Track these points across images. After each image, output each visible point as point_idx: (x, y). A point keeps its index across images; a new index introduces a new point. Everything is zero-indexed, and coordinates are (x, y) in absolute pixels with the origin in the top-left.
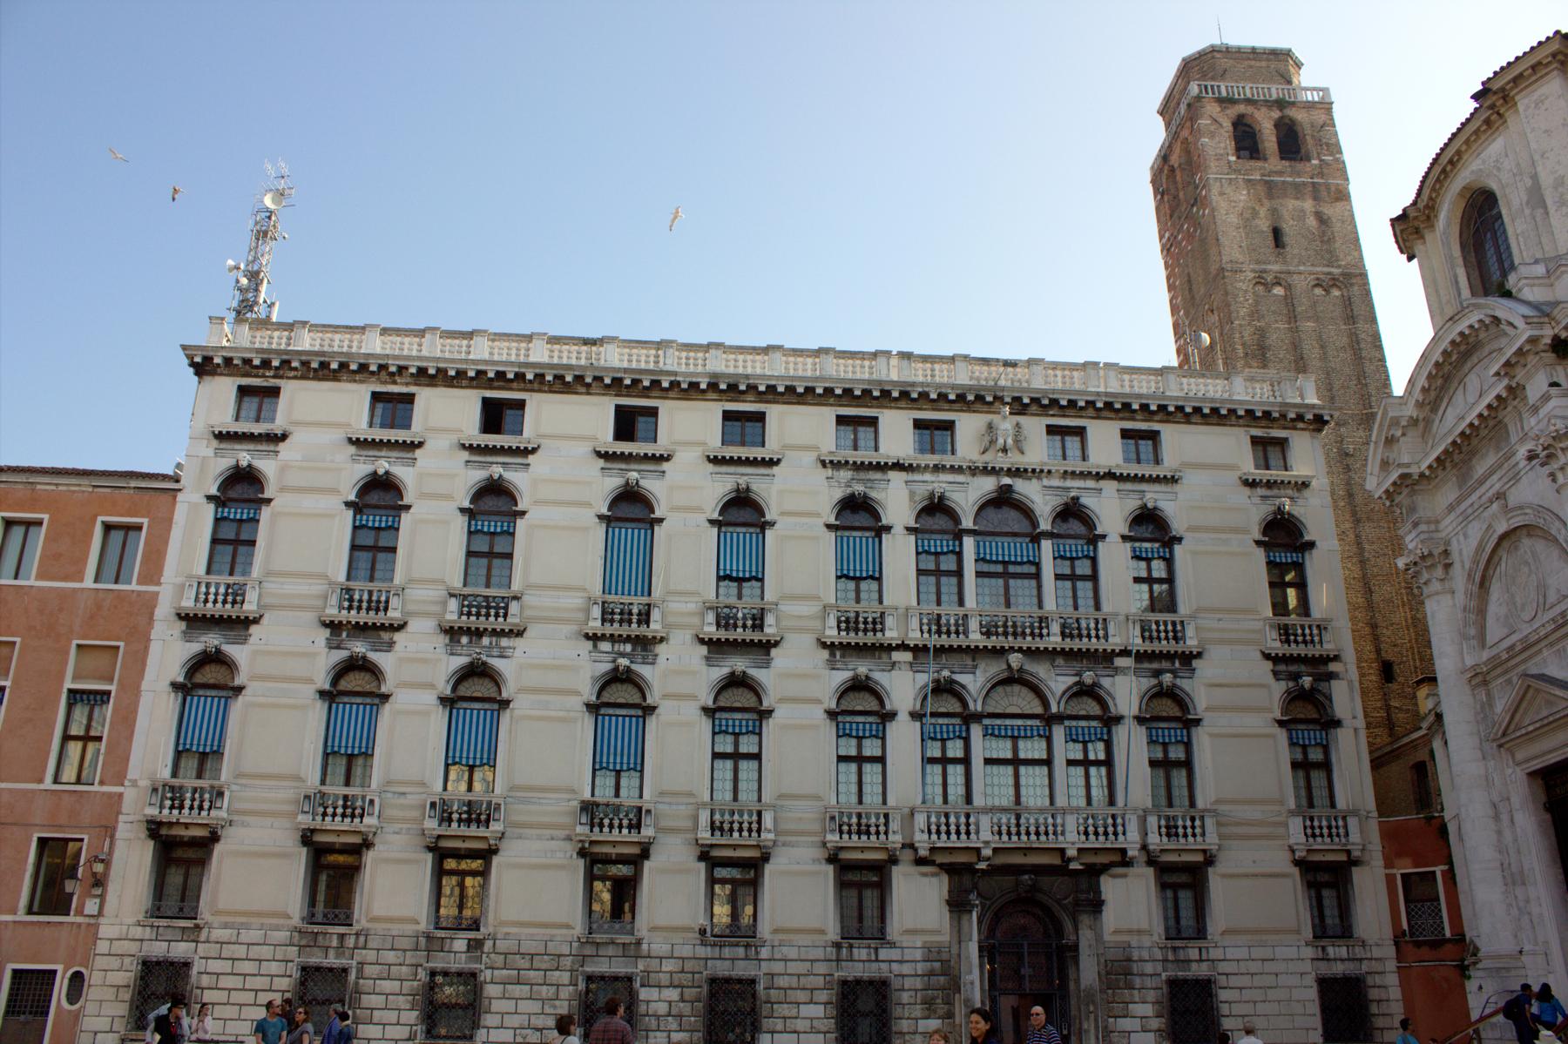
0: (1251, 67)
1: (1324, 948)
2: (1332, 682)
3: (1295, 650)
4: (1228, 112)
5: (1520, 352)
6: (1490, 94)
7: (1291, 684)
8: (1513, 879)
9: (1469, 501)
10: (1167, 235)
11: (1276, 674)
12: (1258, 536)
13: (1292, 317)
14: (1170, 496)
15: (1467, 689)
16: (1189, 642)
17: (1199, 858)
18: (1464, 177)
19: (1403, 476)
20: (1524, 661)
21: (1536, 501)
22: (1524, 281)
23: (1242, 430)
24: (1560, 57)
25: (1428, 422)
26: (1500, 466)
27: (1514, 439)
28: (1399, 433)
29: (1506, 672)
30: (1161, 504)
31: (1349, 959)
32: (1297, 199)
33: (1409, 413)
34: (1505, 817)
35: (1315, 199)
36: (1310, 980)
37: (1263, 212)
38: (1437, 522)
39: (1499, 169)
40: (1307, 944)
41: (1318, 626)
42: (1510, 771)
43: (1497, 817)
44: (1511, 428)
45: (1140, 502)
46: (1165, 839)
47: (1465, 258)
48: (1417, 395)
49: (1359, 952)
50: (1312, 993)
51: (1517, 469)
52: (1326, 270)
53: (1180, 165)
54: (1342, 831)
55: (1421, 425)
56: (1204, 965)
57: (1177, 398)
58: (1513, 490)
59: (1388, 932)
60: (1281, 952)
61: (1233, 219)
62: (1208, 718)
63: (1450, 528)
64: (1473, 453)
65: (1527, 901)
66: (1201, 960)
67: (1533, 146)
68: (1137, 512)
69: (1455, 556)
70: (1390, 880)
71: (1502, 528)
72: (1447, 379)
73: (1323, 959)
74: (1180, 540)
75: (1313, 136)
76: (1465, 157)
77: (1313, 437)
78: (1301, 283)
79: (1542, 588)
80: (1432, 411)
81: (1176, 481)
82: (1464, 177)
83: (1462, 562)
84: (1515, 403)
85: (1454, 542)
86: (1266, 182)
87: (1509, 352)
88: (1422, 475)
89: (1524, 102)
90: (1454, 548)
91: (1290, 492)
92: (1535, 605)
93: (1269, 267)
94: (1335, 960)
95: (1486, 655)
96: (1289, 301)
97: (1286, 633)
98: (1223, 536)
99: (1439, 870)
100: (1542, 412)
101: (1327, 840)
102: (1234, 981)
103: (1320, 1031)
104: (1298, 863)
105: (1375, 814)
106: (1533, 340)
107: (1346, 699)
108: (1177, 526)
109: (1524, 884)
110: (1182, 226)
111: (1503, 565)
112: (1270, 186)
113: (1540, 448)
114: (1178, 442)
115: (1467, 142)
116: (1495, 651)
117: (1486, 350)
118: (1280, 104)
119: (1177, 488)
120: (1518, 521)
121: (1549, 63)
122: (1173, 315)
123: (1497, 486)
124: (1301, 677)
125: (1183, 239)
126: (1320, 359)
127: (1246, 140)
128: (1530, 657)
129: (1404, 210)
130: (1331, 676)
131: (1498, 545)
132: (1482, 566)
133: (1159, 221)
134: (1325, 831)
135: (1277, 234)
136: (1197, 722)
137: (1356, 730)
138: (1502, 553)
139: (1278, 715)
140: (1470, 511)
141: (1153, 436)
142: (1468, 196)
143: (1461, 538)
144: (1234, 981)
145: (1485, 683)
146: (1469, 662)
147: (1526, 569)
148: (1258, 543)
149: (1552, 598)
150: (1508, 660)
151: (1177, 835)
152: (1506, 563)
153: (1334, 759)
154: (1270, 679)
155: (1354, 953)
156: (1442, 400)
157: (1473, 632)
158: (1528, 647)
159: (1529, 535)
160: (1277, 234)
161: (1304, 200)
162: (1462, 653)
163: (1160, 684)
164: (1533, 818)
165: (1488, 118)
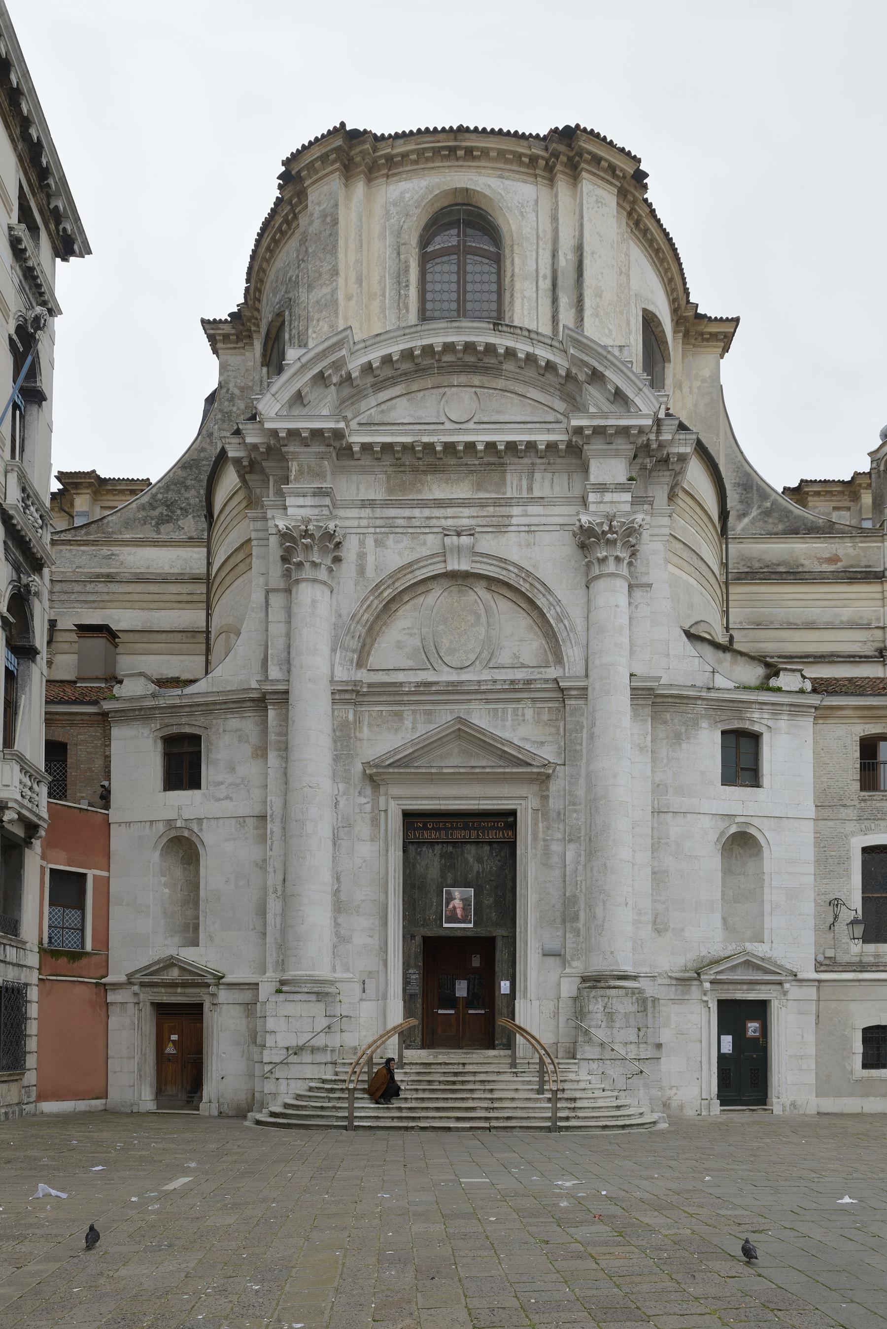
8: (339, 907)
9: (407, 513)
15: (330, 697)
25: (358, 395)
26: (482, 506)
55: (347, 391)
63: (355, 523)
70: (42, 868)
72: (421, 371)
92: (473, 657)
94: (9, 963)
123: (465, 522)
131: (434, 578)
132: (401, 585)
140: (401, 522)
146: (341, 674)
147: (471, 618)
149: (504, 658)
158: (454, 690)
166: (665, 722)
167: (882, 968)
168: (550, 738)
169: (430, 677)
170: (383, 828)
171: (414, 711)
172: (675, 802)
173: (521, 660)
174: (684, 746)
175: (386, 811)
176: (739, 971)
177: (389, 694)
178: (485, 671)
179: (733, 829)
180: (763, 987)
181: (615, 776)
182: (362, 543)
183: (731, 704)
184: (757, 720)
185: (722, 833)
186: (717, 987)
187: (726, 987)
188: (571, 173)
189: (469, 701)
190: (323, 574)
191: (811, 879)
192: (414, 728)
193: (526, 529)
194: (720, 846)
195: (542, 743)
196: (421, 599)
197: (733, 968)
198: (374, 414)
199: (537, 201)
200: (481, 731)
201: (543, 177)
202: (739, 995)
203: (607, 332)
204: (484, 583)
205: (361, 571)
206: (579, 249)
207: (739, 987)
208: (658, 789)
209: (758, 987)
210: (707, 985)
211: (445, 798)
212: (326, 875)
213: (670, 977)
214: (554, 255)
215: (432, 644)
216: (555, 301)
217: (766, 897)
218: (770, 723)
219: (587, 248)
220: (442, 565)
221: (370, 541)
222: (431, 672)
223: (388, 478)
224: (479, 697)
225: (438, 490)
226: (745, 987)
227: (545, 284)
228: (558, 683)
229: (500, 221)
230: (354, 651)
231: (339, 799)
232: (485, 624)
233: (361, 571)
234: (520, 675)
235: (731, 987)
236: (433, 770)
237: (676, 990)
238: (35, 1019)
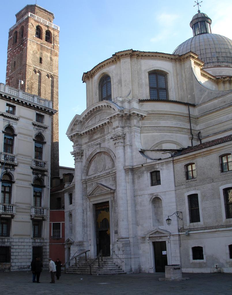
0: (43, 14)
1: (35, 240)
2: (45, 177)
3: (39, 168)
4: (36, 24)
5: (115, 116)
6: (115, 56)
7: (36, 176)
8: (85, 226)
9: (91, 143)
10: (10, 49)
11: (33, 173)
12: (34, 138)
13: (40, 82)
14: (16, 124)
16: (15, 162)
17: (10, 216)
18: (105, 70)
19: (77, 134)
20: (97, 180)
22: (118, 101)
23: (34, 111)
24: (131, 54)
25: (84, 123)
26: (101, 138)
28: (78, 123)
29: (92, 182)
30: (13, 125)
31: (40, 242)
32: (47, 52)
33: (81, 120)
34: (85, 213)
35: (51, 54)
36: (31, 247)
37: (39, 53)
38: (81, 145)
39: (112, 72)
40: (32, 239)
41: (44, 163)
43: (83, 213)
44: (105, 130)
45: (8, 124)
46: (3, 211)
47: (99, 88)
48: (84, 116)
49: (42, 241)
50: (31, 250)
52: (50, 72)
53: (19, 32)
54: (11, 210)
56: (8, 243)
57: (22, 99)
58: (102, 143)
59: (48, 236)
60: (26, 240)
61: (31, 52)
62: (16, 181)
63: (85, 148)
64: (94, 133)
65: (87, 231)
66: (8, 242)
67: (122, 71)
68: (7, 126)
69: (84, 154)
70: (50, 224)
71: (98, 151)
72: (92, 114)
73: (34, 242)
74: (16, 135)
75: (54, 38)
76: (105, 66)
77: (50, 117)
78: (44, 74)
79: (105, 166)
80: (86, 120)
81: (47, 128)
82: (105, 70)
83: (86, 156)
84: (108, 125)
85: (85, 151)
86: (41, 45)
87: (112, 115)
88: (81, 134)
89: (122, 61)
90: (85, 152)
91: (42, 129)
93: (37, 67)
94: (37, 242)
95: (88, 177)
96: (40, 77)
97: (37, 163)
98: (26, 137)
99: (61, 223)
100: (116, 130)
101: (39, 214)
102: (15, 247)
103: (32, 259)
104: (32, 219)
105: (49, 209)
106: (118, 114)
107: (47, 181)
108: (16, 132)
109: (87, 227)
110: (16, 48)
111: (96, 159)
112: (42, 47)
113: (114, 137)
114: (20, 110)
115: (107, 63)
116: (90, 177)
117: (103, 111)
118: (48, 27)
119: (17, 122)
120: (102, 150)
122: (7, 70)
123: (99, 142)
124: (39, 174)
125: (15, 52)
126: (44, 94)
127: (39, 33)
128: (98, 180)
129: (87, 72)
130: (45, 175)
132: (91, 158)
133: (9, 44)
134: (39, 212)
135: (41, 59)
136: (14, 182)
137: (48, 189)
138: (97, 156)
139: (32, 183)
140: (91, 145)
141: (14, 107)
143: (87, 150)
144: (15, 247)
145: (86, 183)
146: (83, 178)
148: (34, 140)
149: (107, 168)
150: (93, 179)
151: (6, 210)
152: (97, 158)
153: (42, 195)
154: (32, 174)
155: (41, 241)
156: (89, 119)
157: (85, 171)
159: (104, 154)
160: (41, 59)
161: (48, 53)
162: (82, 177)
163: (7, 171)
164: (92, 214)
165: (113, 60)
166: (136, 174)
167: (195, 230)
168: (114, 184)
169: (96, 175)
172: (139, 193)
174: (141, 179)
176: (157, 233)
179: (154, 197)
180: (163, 238)
183: (151, 166)
184: (158, 168)
185: (151, 198)
186: (151, 238)
187: (154, 238)
189: (102, 179)
191: (175, 207)
193: (108, 140)
194: (151, 202)
195: (113, 185)
197: (155, 233)
198: (87, 126)
202: (157, 240)
207: (157, 238)
208: (134, 191)
209: (162, 238)
210: (148, 238)
211: (98, 200)
212: (81, 220)
213: (141, 237)
217: (163, 213)
218: (161, 168)
223: (89, 137)
226: (159, 238)
235: (155, 238)
237: (142, 240)
238: (48, 252)
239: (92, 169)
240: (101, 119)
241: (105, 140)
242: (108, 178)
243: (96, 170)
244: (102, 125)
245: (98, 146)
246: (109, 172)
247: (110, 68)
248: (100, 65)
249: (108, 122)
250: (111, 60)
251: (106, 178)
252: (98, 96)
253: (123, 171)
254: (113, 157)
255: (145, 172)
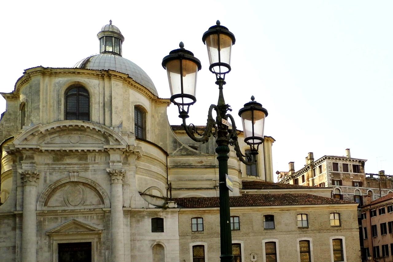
21: (93, 179)
27: (89, 161)
39: (95, 88)
42: (47, 241)
51: (88, 169)
84: (97, 154)
100: (115, 164)
106: (123, 148)
113: (114, 172)
115: (88, 74)
117: (86, 134)
121: (122, 79)
123: (76, 168)
142: (77, 83)
147: (78, 193)
149: (88, 203)
152: (67, 187)
158: (73, 211)
159: (83, 185)
169: (66, 208)
170: (52, 249)
171: (61, 217)
173: (93, 203)
175: (53, 244)
177: (54, 213)
178: (82, 206)
181: (118, 233)
182: (45, 174)
188: (108, 78)
190: (33, 183)
192: (61, 221)
196: (64, 188)
199: (99, 84)
200: (80, 222)
201: (101, 78)
203: (119, 117)
204: (82, 184)
205: (45, 181)
206: (111, 97)
214: (104, 98)
215: (67, 200)
216: (104, 109)
219: (113, 97)
220: (69, 180)
221: (48, 174)
222: (67, 207)
224: (80, 213)
225: (68, 160)
227: (101, 105)
228: (103, 209)
229: (88, 89)
230: (43, 202)
231: (38, 241)
232: (82, 194)
233: (45, 181)
234: (92, 207)
236: (67, 233)
239: (57, 199)
240: (80, 142)
241: (88, 169)
242: (90, 215)
243: (66, 202)
244: (89, 151)
245: (75, 174)
246: (94, 209)
247: (91, 80)
248: (75, 69)
249: (100, 151)
250: (96, 73)
251: (87, 215)
252: (62, 107)
253: (122, 212)
254: (103, 193)
255: (146, 217)
